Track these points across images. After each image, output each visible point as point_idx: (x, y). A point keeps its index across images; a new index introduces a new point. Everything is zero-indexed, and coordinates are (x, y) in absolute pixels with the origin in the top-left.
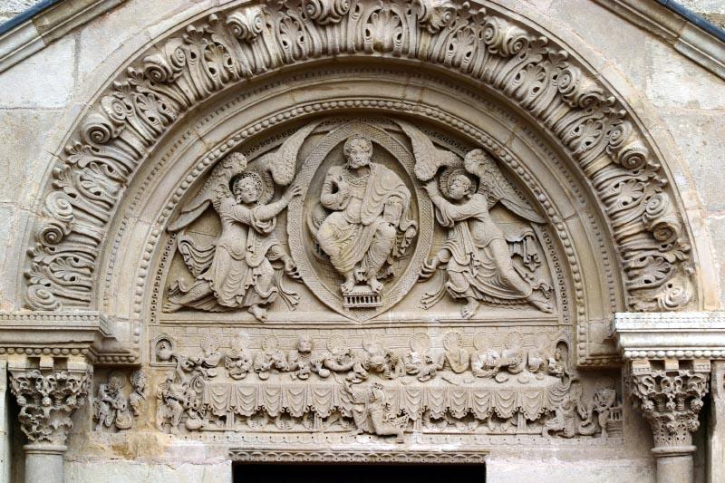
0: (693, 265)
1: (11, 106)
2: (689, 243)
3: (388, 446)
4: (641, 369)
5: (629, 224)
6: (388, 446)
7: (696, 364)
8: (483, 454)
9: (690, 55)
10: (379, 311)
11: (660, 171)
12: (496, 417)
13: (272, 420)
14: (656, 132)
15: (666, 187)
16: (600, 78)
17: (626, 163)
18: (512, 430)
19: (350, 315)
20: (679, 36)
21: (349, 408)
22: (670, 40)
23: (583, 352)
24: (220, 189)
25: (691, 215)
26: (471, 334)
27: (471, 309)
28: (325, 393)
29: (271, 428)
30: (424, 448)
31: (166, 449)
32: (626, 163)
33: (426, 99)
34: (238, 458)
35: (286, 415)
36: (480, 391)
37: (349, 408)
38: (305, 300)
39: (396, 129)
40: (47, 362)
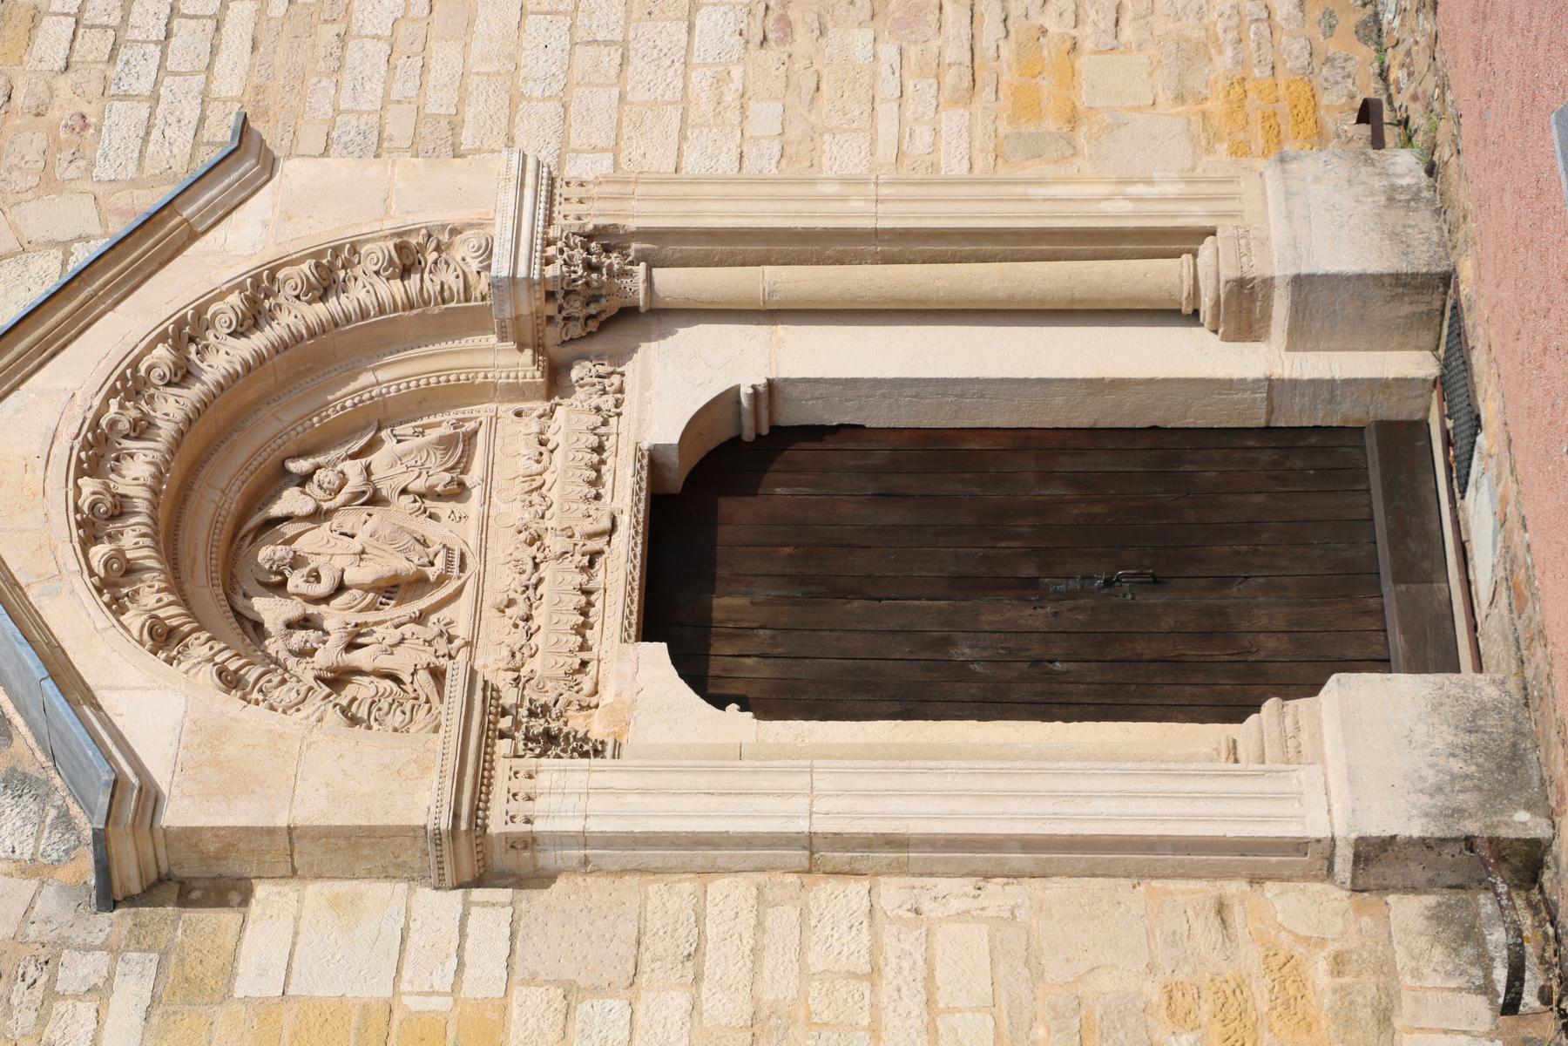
0: (443, 227)
1: (175, 745)
2: (418, 230)
3: (624, 522)
4: (551, 271)
5: (393, 290)
6: (624, 522)
7: (551, 235)
8: (638, 449)
9: (210, 221)
10: (465, 548)
11: (336, 251)
12: (599, 449)
13: (590, 604)
14: (293, 249)
15: (354, 250)
16: (224, 288)
17: (325, 285)
18: (613, 439)
19: (467, 573)
20: (186, 220)
21: (578, 557)
22: (193, 237)
23: (529, 374)
24: (302, 666)
25: (389, 225)
26: (499, 480)
27: (469, 480)
28: (560, 580)
29: (597, 627)
30: (629, 492)
31: (619, 694)
32: (325, 285)
33: (222, 485)
34: (633, 631)
35: (581, 630)
36: (566, 456)
37: (578, 557)
38: (446, 613)
39: (250, 538)
40: (505, 723)
